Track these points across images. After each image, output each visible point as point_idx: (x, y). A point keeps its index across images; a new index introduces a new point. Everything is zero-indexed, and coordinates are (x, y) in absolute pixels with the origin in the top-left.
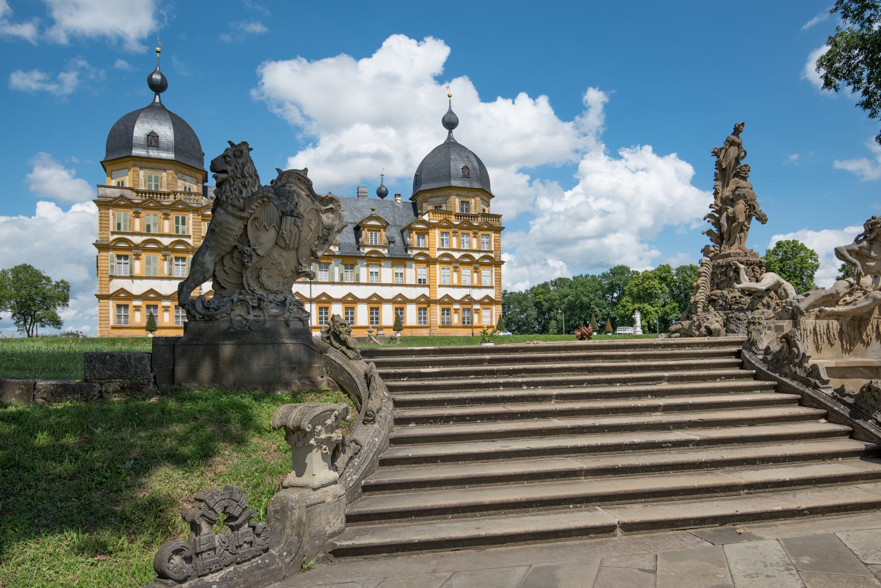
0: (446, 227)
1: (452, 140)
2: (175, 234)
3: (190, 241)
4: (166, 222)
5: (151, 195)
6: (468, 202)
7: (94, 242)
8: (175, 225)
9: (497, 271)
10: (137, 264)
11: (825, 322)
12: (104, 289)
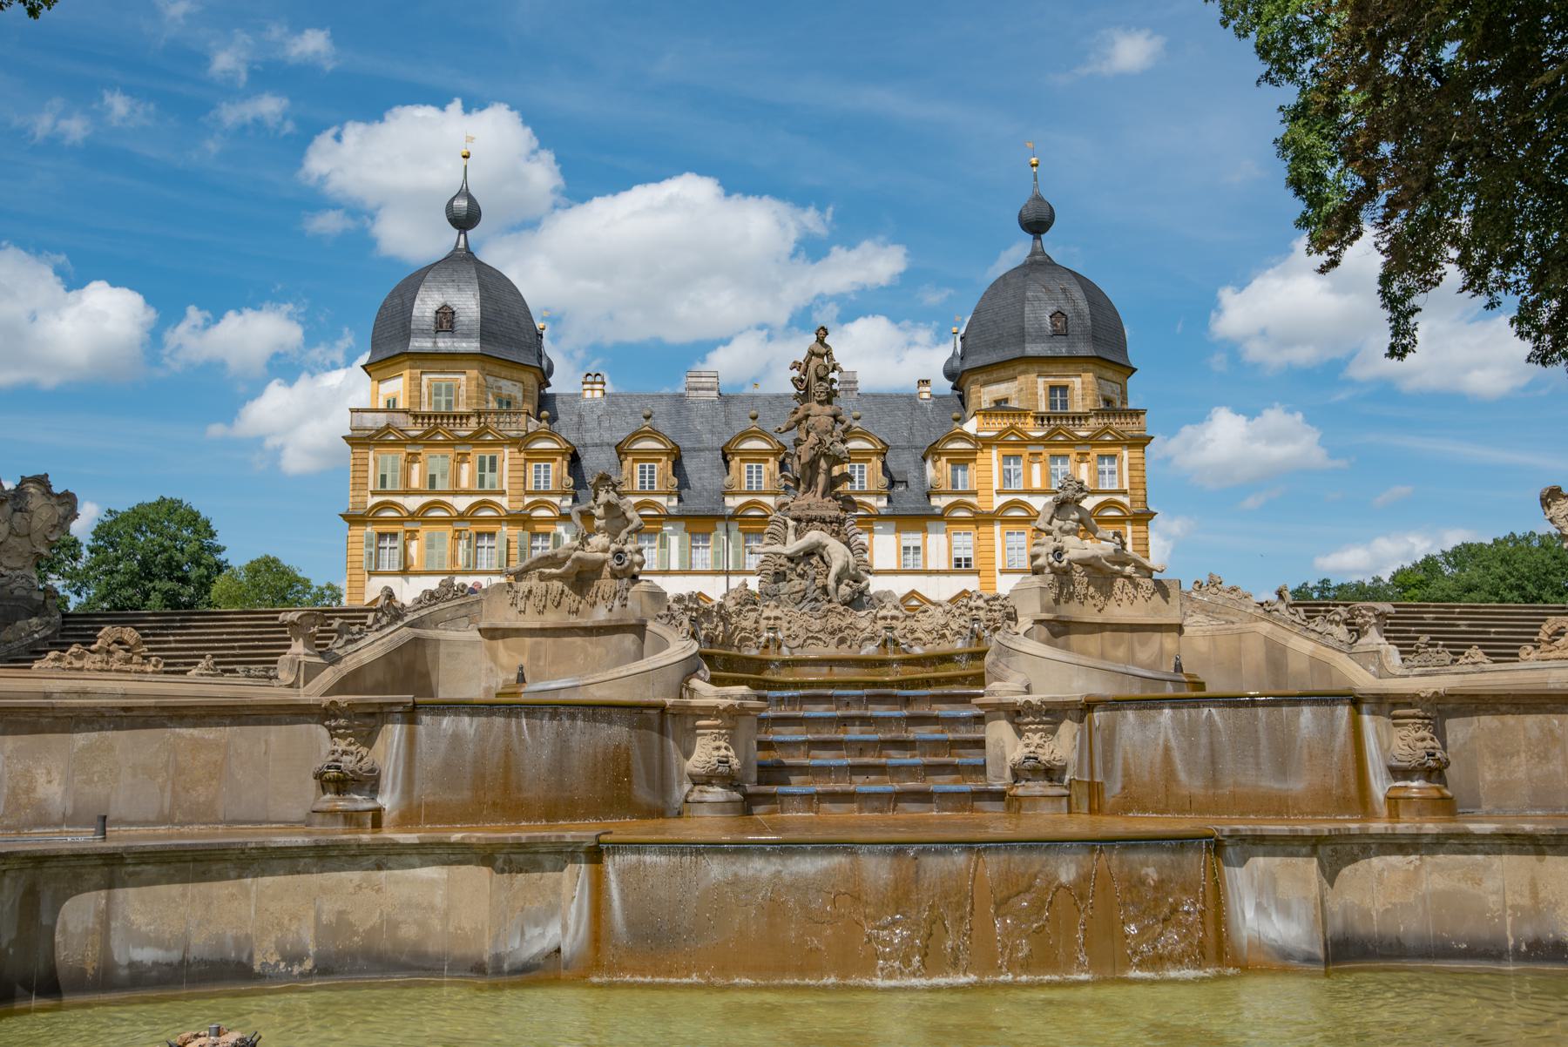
0: (1011, 444)
1: (1038, 258)
2: (477, 489)
3: (504, 501)
5: (439, 421)
6: (1067, 386)
7: (343, 512)
8: (478, 474)
9: (1137, 535)
11: (543, 584)
12: (354, 597)
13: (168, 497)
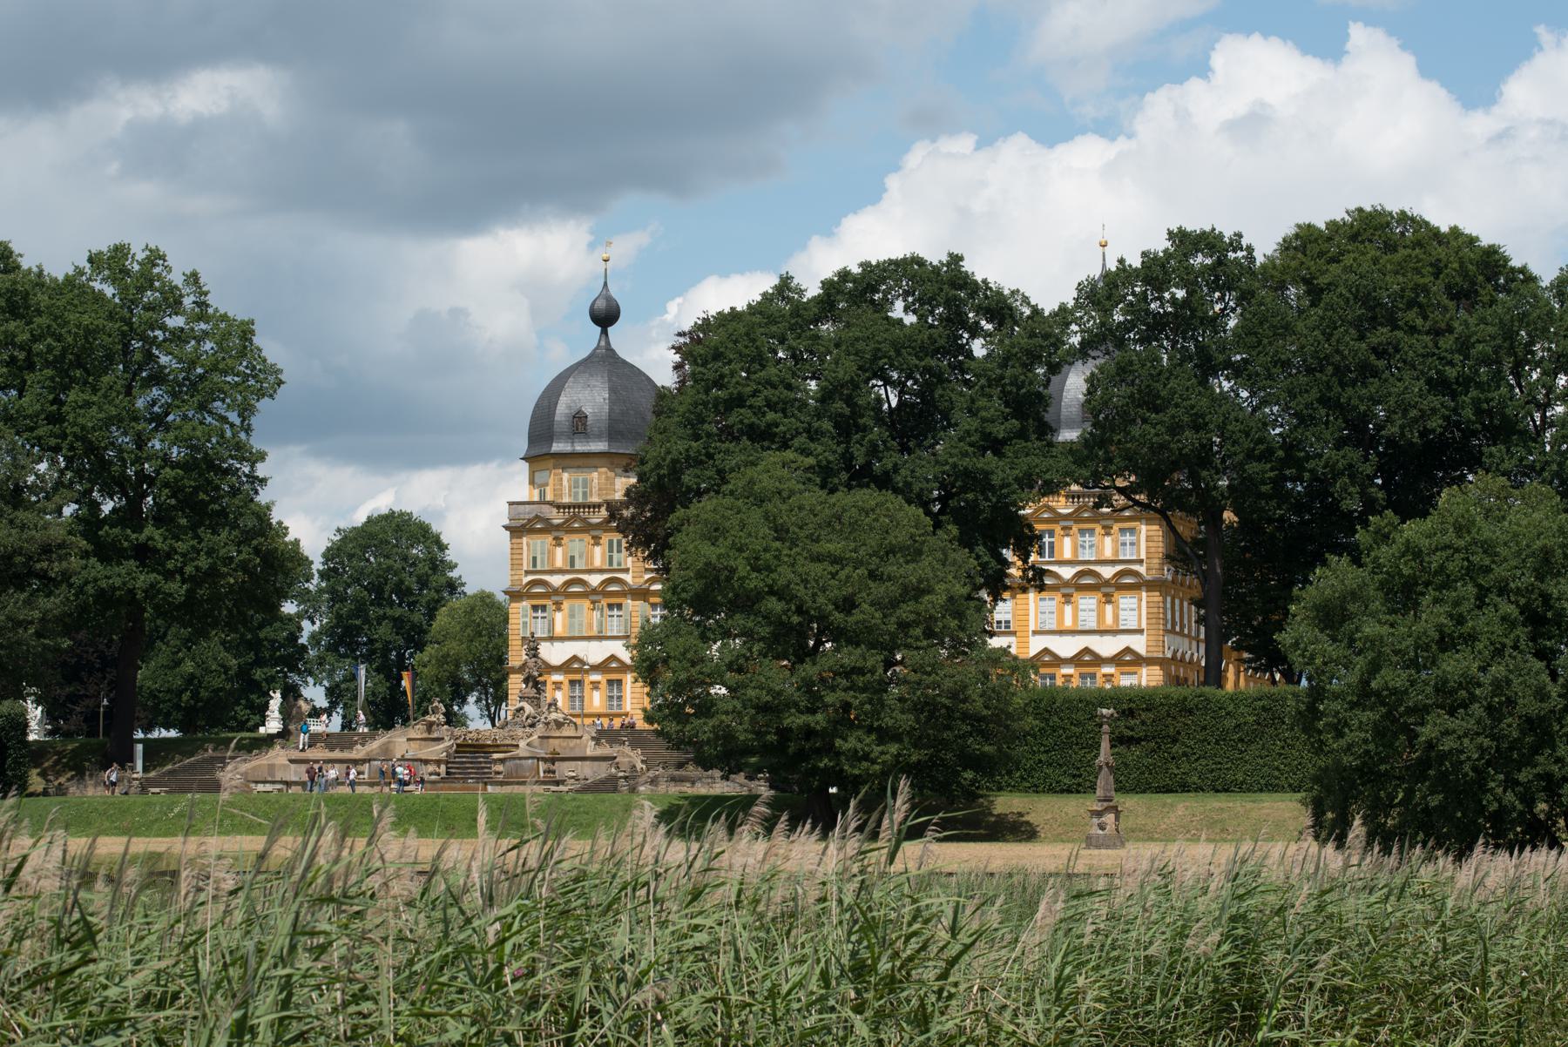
2: (607, 567)
3: (628, 578)
4: (598, 550)
10: (559, 617)
13: (396, 509)
